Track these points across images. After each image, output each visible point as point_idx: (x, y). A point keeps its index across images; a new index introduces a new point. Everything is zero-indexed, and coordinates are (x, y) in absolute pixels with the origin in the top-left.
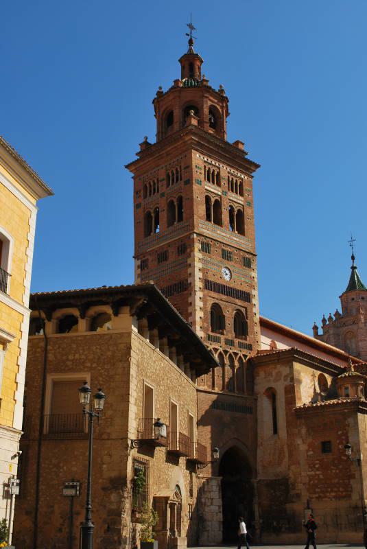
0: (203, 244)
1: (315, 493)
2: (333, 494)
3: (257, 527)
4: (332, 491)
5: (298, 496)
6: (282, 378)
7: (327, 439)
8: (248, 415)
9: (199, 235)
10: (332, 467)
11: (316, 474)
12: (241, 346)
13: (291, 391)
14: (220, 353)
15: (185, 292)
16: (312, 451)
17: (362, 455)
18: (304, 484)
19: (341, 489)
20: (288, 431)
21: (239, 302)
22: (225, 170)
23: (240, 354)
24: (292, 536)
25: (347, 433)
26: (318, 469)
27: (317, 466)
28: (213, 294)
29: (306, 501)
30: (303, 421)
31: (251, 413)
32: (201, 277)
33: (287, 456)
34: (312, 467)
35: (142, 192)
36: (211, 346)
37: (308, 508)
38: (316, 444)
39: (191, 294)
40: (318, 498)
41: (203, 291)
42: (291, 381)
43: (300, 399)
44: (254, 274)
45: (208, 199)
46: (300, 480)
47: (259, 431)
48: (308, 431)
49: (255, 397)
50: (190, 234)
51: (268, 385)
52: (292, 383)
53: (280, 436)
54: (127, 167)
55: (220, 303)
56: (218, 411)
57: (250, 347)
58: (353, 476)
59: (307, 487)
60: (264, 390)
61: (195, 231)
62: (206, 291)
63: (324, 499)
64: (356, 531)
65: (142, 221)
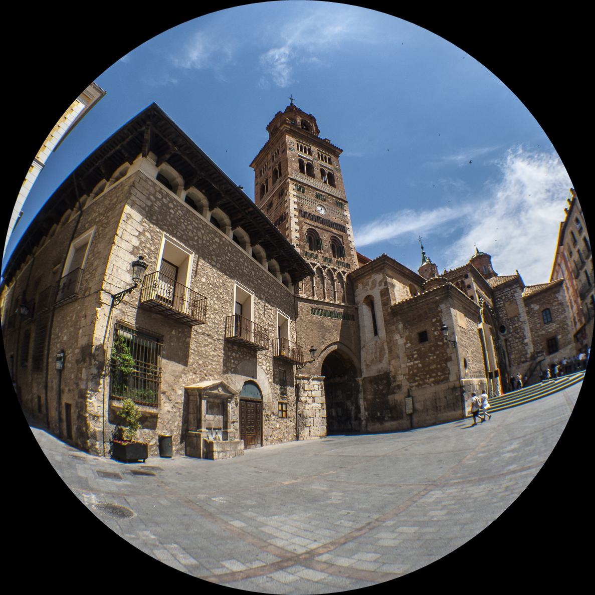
0: (297, 186)
1: (415, 381)
2: (432, 379)
3: (362, 419)
4: (431, 377)
5: (399, 387)
6: (378, 285)
7: (422, 329)
8: (350, 322)
9: (292, 179)
10: (430, 354)
11: (414, 364)
12: (339, 264)
13: (385, 293)
14: (318, 268)
15: (284, 221)
16: (410, 343)
17: (456, 337)
18: (404, 375)
19: (439, 374)
20: (386, 332)
21: (335, 231)
22: (314, 149)
23: (339, 270)
24: (394, 424)
25: (440, 319)
26: (416, 359)
27: (415, 356)
28: (308, 221)
29: (407, 391)
30: (399, 318)
31: (354, 320)
32: (296, 207)
33: (387, 352)
34: (410, 357)
35: (259, 175)
36: (309, 261)
37: (409, 396)
38: (413, 336)
39: (288, 221)
40: (417, 386)
41: (298, 218)
42: (385, 286)
43: (395, 300)
44: (346, 213)
45: (301, 162)
46: (400, 372)
47: (361, 335)
48: (404, 326)
49: (356, 307)
50: (286, 180)
51: (365, 295)
52: (386, 287)
53: (380, 336)
54: (250, 166)
55: (317, 229)
56: (319, 317)
57: (348, 266)
58: (450, 359)
59: (407, 377)
60: (363, 299)
61: (289, 176)
62: (302, 219)
63: (423, 386)
64: (454, 410)
65: (259, 191)
